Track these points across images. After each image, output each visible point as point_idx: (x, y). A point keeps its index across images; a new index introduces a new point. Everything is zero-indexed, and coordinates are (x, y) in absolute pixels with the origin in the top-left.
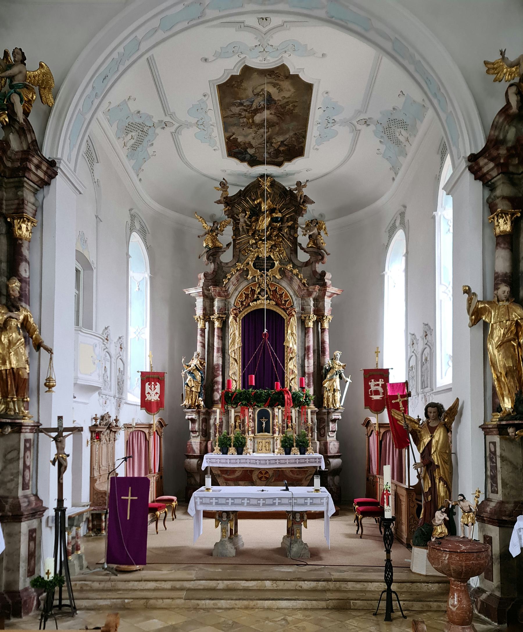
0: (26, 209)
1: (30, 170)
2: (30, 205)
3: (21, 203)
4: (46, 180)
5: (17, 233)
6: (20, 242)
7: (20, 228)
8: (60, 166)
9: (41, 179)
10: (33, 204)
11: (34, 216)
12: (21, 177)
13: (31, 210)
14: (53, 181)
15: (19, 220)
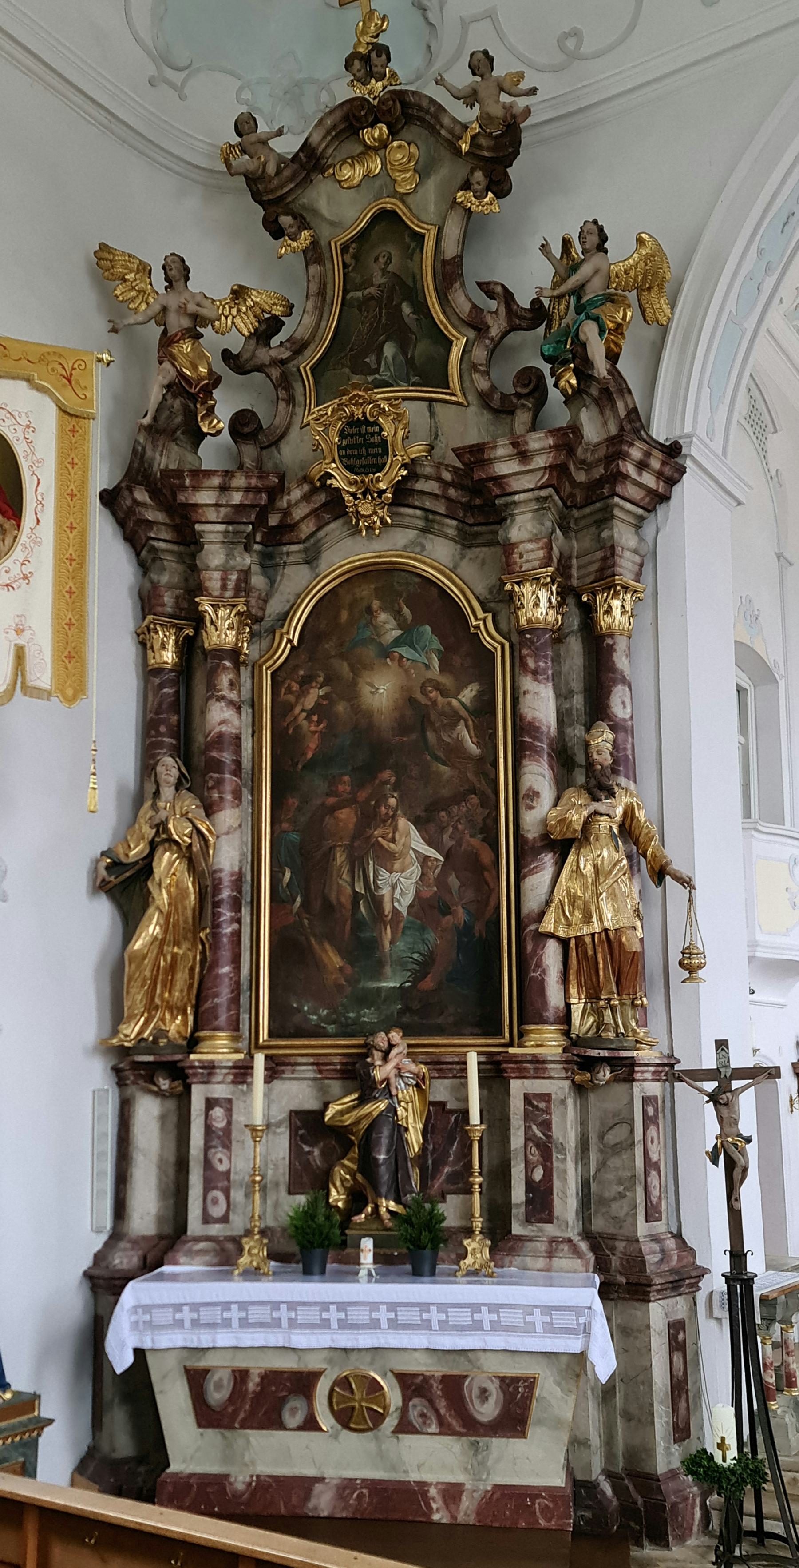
0: (620, 566)
1: (626, 477)
2: (627, 554)
3: (610, 552)
4: (660, 490)
5: (602, 623)
6: (609, 641)
7: (609, 611)
8: (690, 450)
9: (650, 491)
10: (636, 552)
11: (638, 577)
12: (607, 497)
13: (629, 565)
14: (676, 489)
15: (605, 595)
